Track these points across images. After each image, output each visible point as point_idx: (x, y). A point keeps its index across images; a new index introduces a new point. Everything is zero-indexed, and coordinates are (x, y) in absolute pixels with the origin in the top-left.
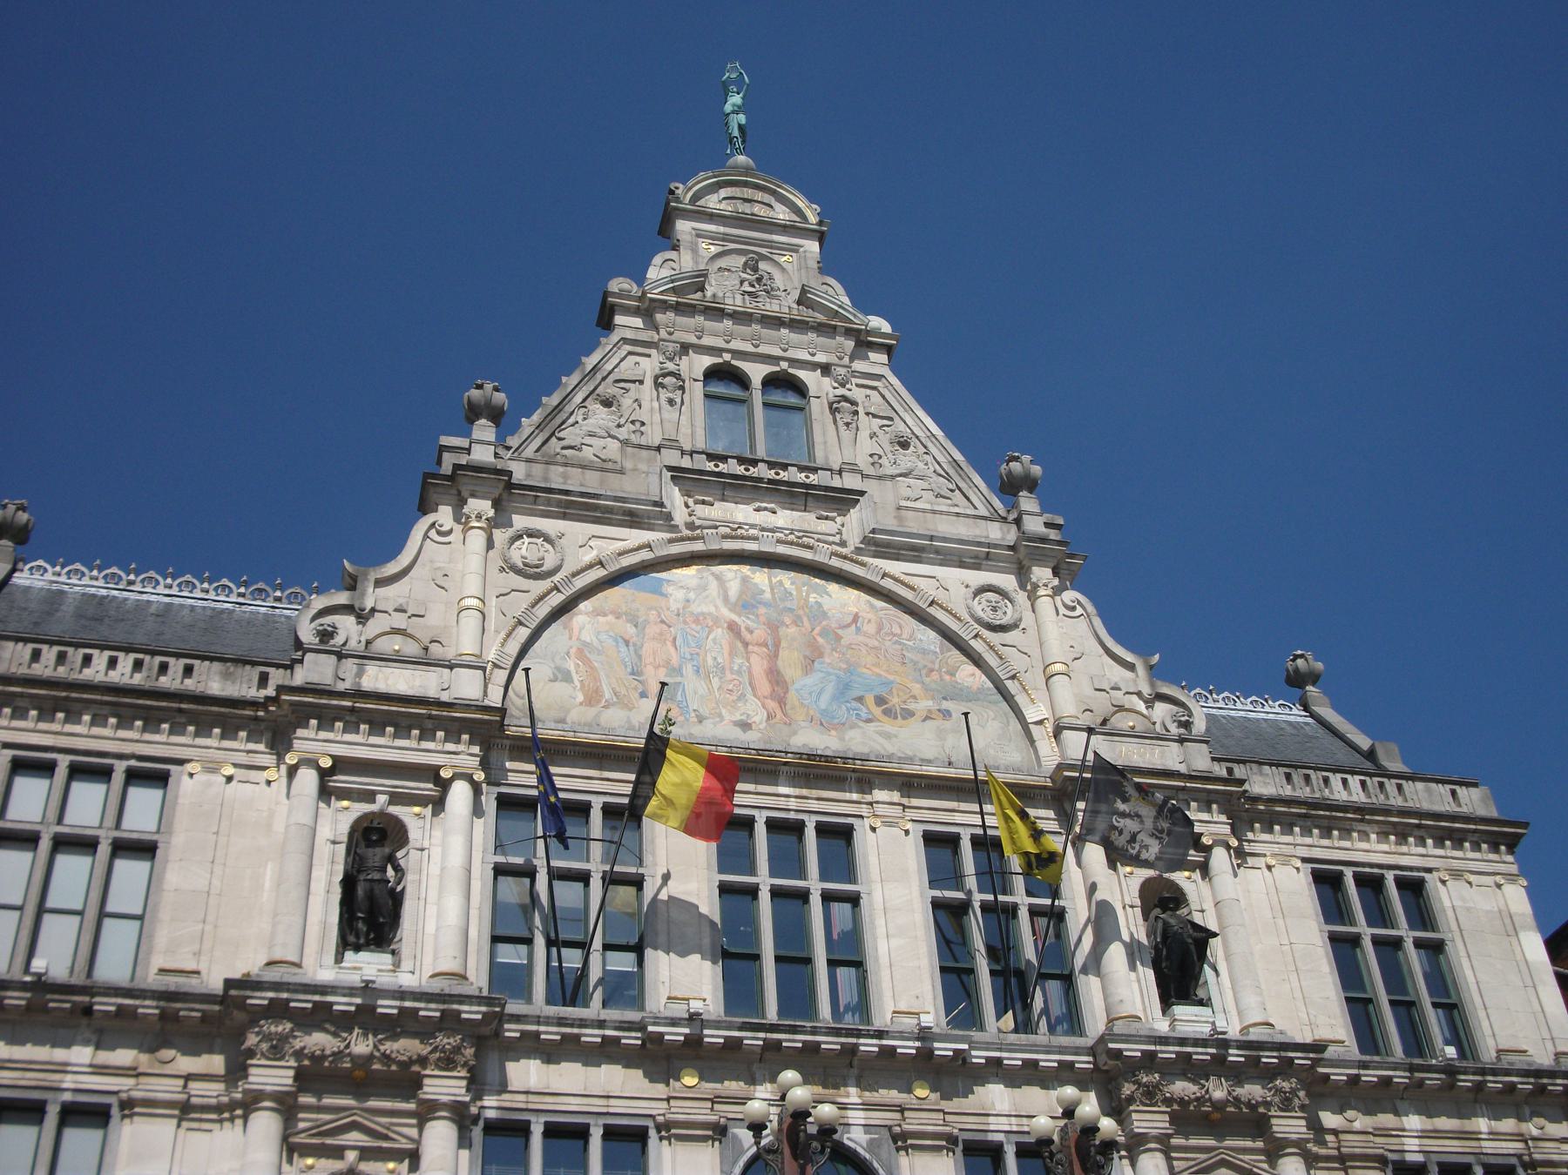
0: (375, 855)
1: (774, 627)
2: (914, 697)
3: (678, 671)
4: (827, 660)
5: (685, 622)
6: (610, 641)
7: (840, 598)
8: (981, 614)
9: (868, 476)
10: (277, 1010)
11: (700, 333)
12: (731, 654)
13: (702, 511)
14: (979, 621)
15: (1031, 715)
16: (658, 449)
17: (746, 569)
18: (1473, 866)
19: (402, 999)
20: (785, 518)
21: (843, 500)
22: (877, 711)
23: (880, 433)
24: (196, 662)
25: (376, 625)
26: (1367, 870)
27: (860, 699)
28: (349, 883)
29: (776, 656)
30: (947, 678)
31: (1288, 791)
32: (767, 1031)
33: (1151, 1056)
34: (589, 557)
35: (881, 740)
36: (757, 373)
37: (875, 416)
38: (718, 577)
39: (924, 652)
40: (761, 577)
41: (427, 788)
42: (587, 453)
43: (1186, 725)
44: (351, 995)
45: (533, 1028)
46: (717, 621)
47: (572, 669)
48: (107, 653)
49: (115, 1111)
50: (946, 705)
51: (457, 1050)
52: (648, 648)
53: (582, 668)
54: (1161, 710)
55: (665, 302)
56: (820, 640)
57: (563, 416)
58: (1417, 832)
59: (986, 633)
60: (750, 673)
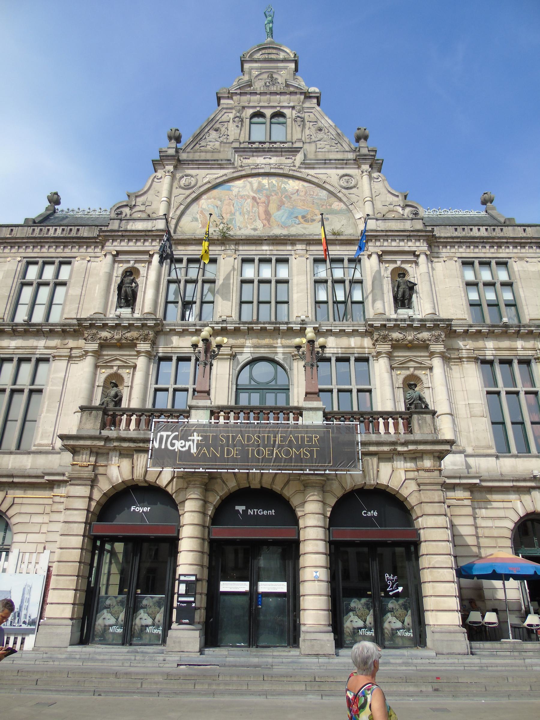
0: (128, 280)
2: (316, 215)
3: (234, 214)
4: (286, 205)
6: (212, 207)
7: (292, 185)
8: (342, 184)
10: (92, 326)
11: (249, 102)
12: (253, 207)
14: (341, 187)
16: (232, 143)
17: (260, 179)
18: (528, 255)
19: (129, 321)
20: (274, 160)
21: (295, 151)
22: (302, 220)
23: (312, 127)
24: (80, 227)
26: (485, 259)
27: (296, 217)
28: (120, 288)
29: (268, 206)
30: (329, 207)
31: (456, 234)
32: (248, 324)
33: (385, 325)
34: (205, 181)
36: (268, 113)
37: (310, 122)
38: (250, 183)
39: (321, 199)
40: (265, 181)
41: (146, 257)
42: (209, 147)
43: (416, 214)
44: (114, 320)
45: (174, 328)
46: (248, 197)
47: (199, 217)
48: (54, 228)
49: (51, 359)
51: (147, 335)
54: (408, 210)
55: (236, 93)
56: (284, 199)
57: (201, 136)
58: (506, 245)
59: (343, 190)
60: (259, 213)
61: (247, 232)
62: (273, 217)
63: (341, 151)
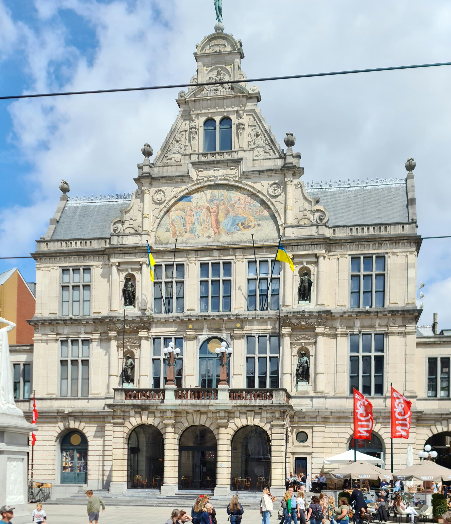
1: (218, 207)
2: (252, 221)
3: (194, 224)
4: (231, 214)
5: (196, 209)
7: (235, 195)
9: (246, 151)
12: (207, 216)
13: (200, 174)
15: (280, 223)
22: (241, 227)
25: (127, 224)
28: (124, 291)
29: (218, 215)
30: (261, 214)
34: (173, 195)
35: (241, 236)
36: (218, 119)
38: (205, 194)
46: (204, 207)
50: (259, 222)
52: (188, 218)
53: (172, 227)
56: (229, 208)
57: (167, 148)
61: (203, 241)
62: (221, 225)
63: (272, 159)
